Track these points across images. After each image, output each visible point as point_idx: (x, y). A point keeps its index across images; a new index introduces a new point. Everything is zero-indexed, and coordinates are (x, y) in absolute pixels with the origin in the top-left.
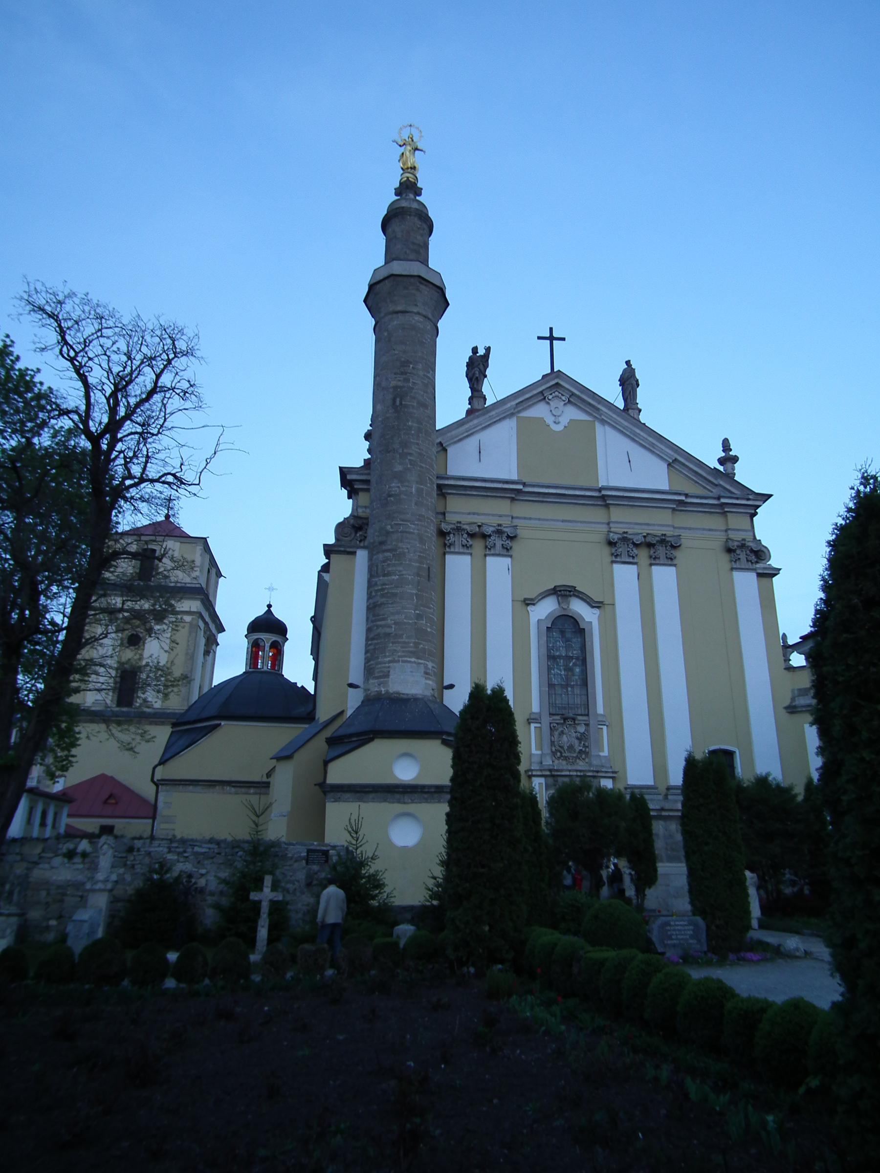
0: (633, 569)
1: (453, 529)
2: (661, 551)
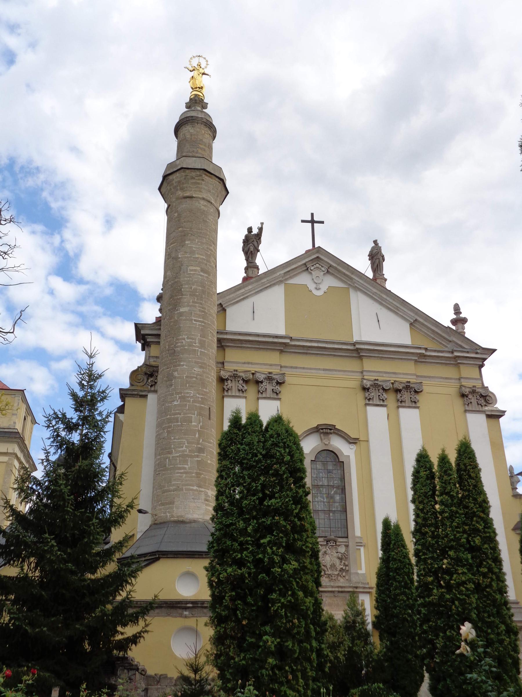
0: (383, 411)
1: (230, 376)
2: (406, 396)
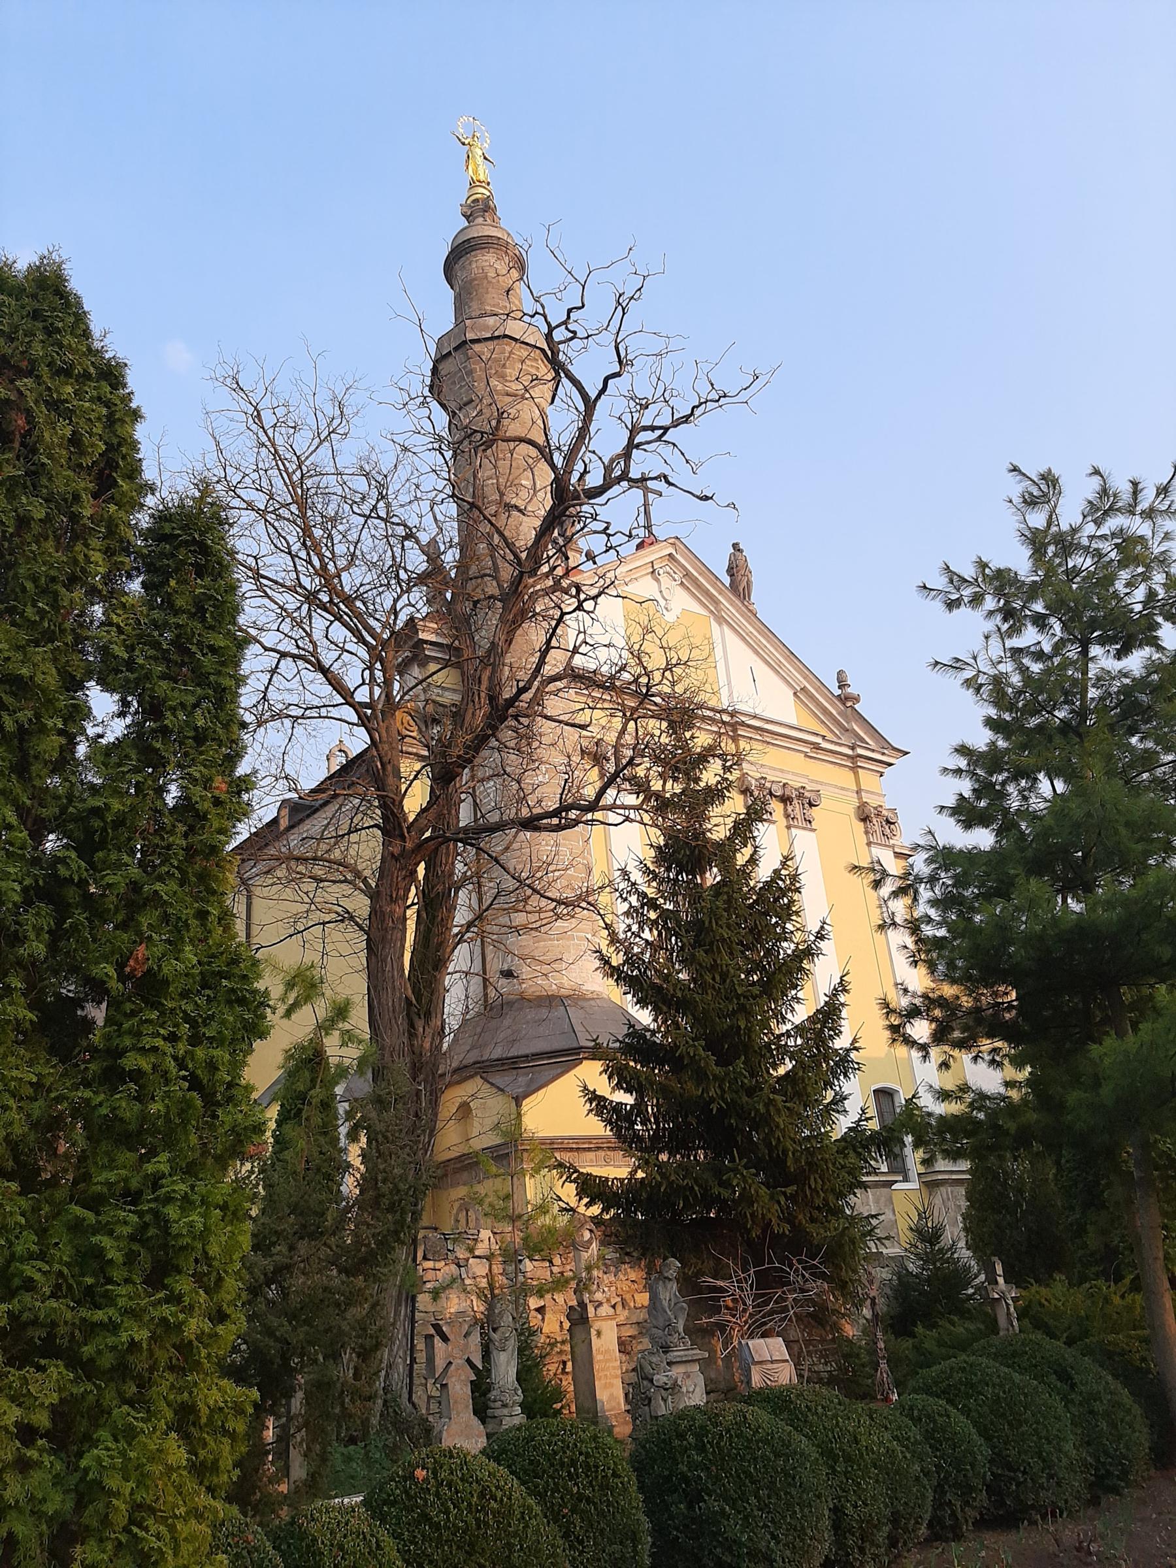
2: (796, 809)
